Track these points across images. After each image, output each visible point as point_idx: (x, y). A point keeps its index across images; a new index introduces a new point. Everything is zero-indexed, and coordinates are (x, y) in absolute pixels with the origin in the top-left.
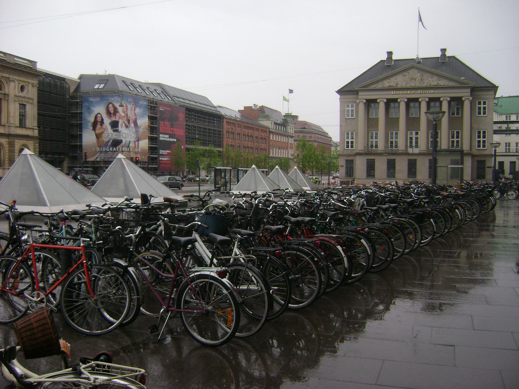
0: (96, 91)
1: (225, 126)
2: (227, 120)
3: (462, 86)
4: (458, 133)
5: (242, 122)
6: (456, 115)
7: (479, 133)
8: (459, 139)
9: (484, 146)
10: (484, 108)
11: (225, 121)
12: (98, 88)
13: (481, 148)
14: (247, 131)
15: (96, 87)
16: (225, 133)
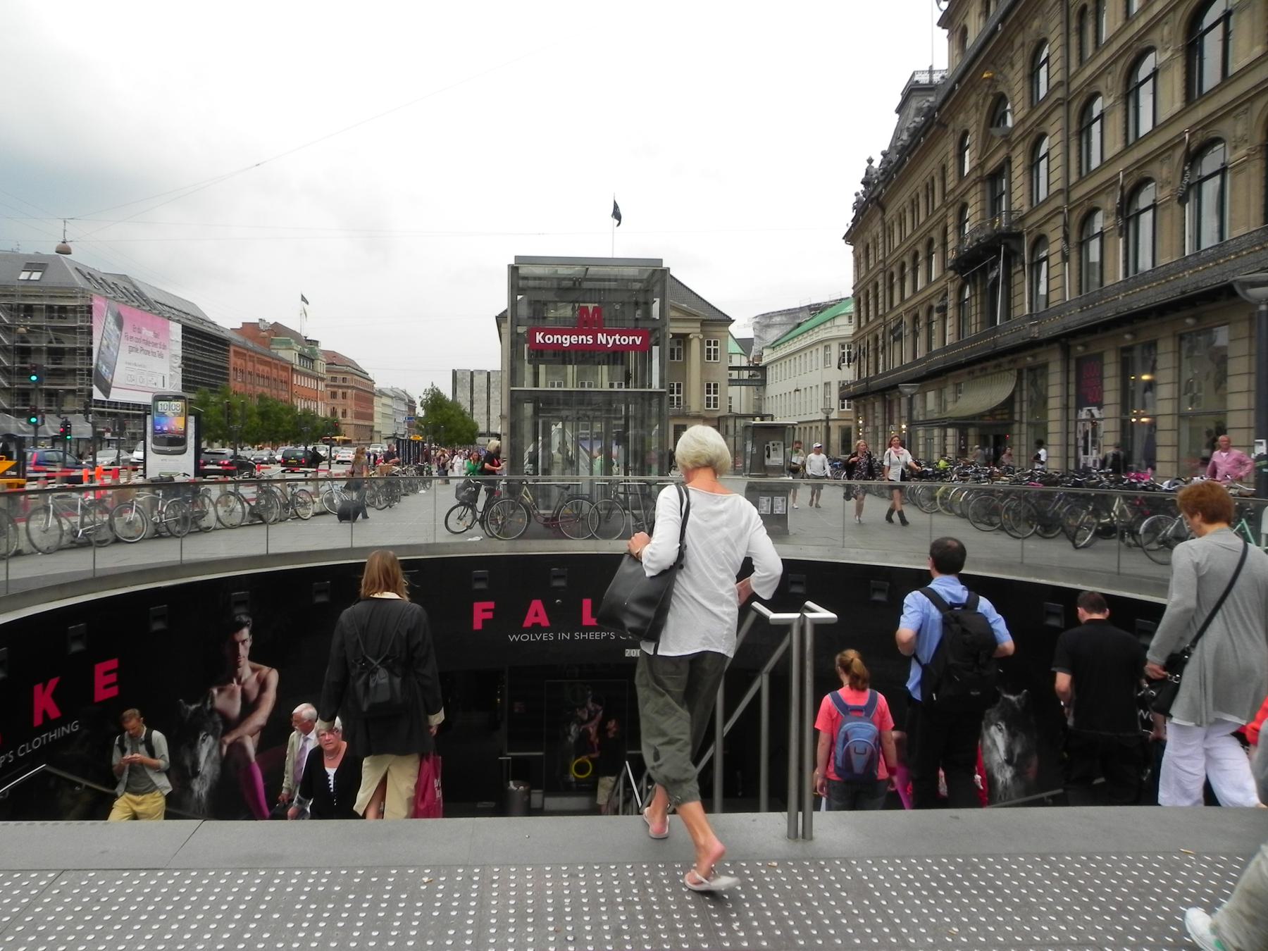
0: (23, 283)
1: (233, 360)
2: (237, 349)
3: (689, 317)
4: (679, 386)
5: (256, 352)
6: (676, 360)
7: (709, 386)
8: (681, 395)
9: (715, 406)
10: (715, 351)
11: (232, 348)
12: (28, 280)
13: (712, 408)
14: (261, 368)
15: (24, 276)
16: (232, 372)
